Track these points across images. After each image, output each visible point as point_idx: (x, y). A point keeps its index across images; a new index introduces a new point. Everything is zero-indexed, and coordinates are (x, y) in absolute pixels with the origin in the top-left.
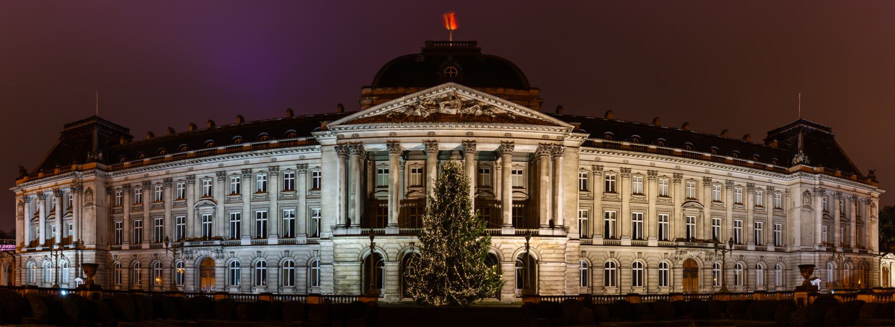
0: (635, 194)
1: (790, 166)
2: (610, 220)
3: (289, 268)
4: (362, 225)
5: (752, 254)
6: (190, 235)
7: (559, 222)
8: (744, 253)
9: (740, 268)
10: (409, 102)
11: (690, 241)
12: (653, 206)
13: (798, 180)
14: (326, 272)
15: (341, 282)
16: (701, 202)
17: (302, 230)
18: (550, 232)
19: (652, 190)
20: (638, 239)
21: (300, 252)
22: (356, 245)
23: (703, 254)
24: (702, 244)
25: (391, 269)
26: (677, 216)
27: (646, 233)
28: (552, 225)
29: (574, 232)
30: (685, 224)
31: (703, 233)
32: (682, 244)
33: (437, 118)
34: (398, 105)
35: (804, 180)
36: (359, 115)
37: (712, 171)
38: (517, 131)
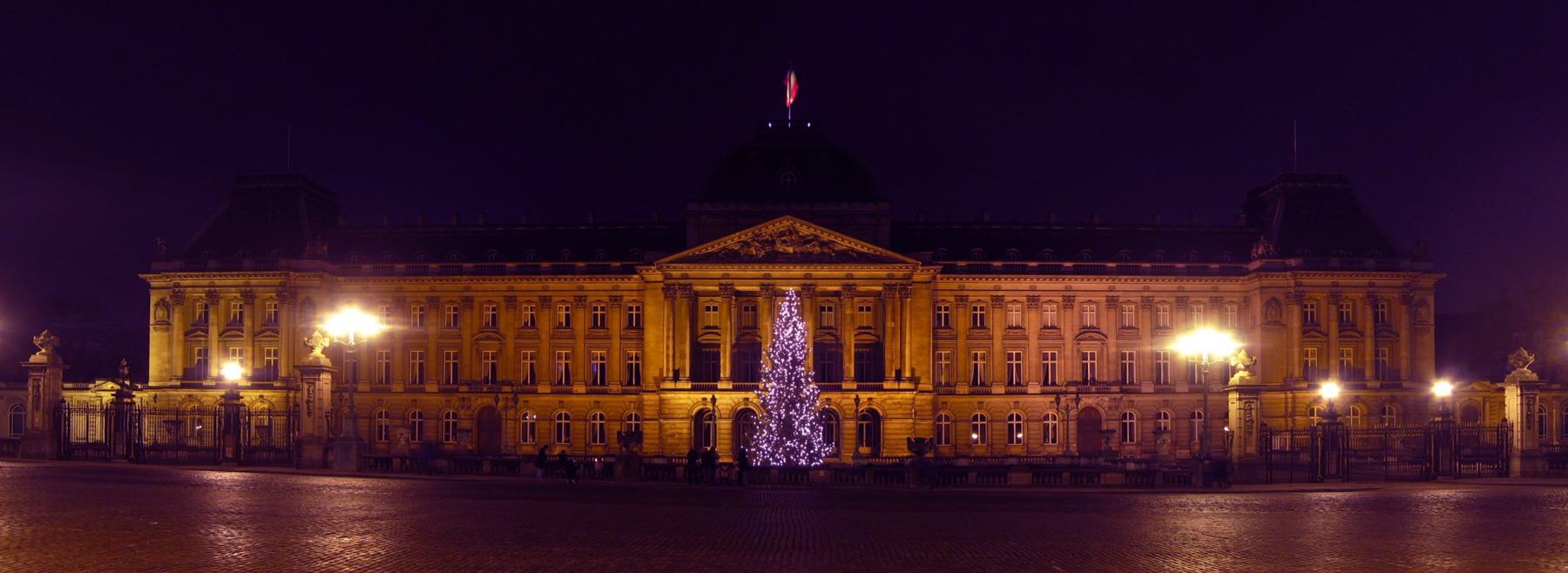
0: (1011, 327)
1: (1249, 261)
2: (980, 363)
3: (598, 422)
4: (692, 378)
5: (1183, 397)
6: (465, 375)
7: (907, 374)
8: (1170, 397)
9: (1166, 417)
10: (743, 238)
11: (1086, 383)
12: (1033, 342)
13: (1257, 284)
14: (650, 429)
15: (670, 441)
16: (1104, 330)
17: (616, 377)
18: (896, 386)
19: (1033, 323)
20: (1015, 386)
21: (616, 403)
22: (686, 400)
23: (1105, 400)
24: (1103, 387)
25: (724, 426)
26: (1068, 353)
27: (1025, 376)
28: (899, 378)
29: (926, 385)
30: (1078, 362)
31: (1105, 373)
32: (1073, 389)
33: (773, 258)
34: (731, 242)
35: (1266, 282)
36: (689, 252)
37: (1119, 286)
38: (861, 271)
